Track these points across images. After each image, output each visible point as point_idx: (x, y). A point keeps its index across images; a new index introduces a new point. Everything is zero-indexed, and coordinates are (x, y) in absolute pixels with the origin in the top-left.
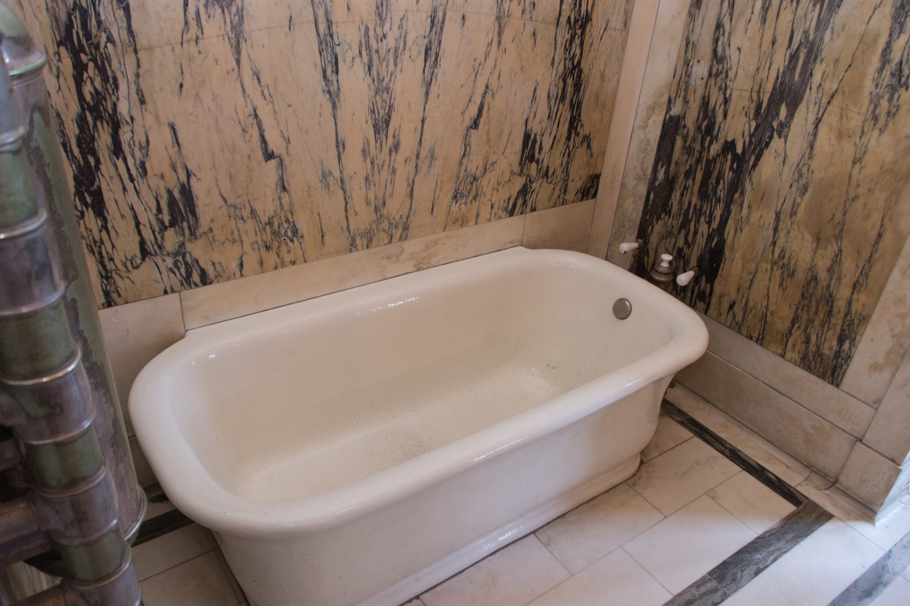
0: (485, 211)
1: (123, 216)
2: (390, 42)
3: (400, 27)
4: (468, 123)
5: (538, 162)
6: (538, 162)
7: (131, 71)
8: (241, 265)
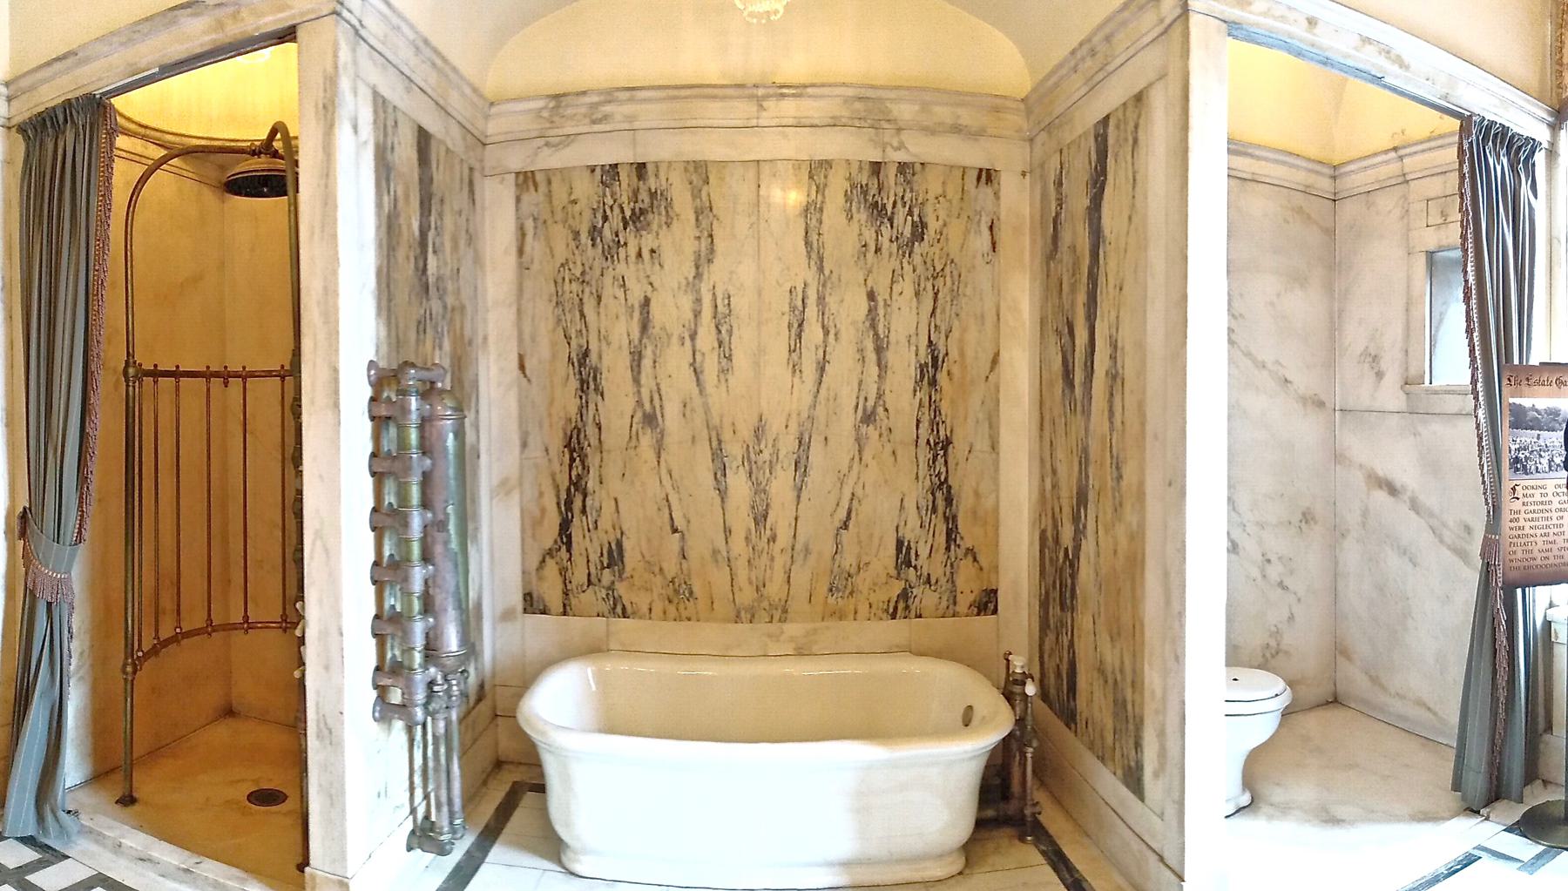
0: (863, 609)
2: (766, 456)
3: (773, 446)
4: (838, 524)
5: (915, 567)
6: (915, 567)
7: (597, 465)
8: (650, 609)
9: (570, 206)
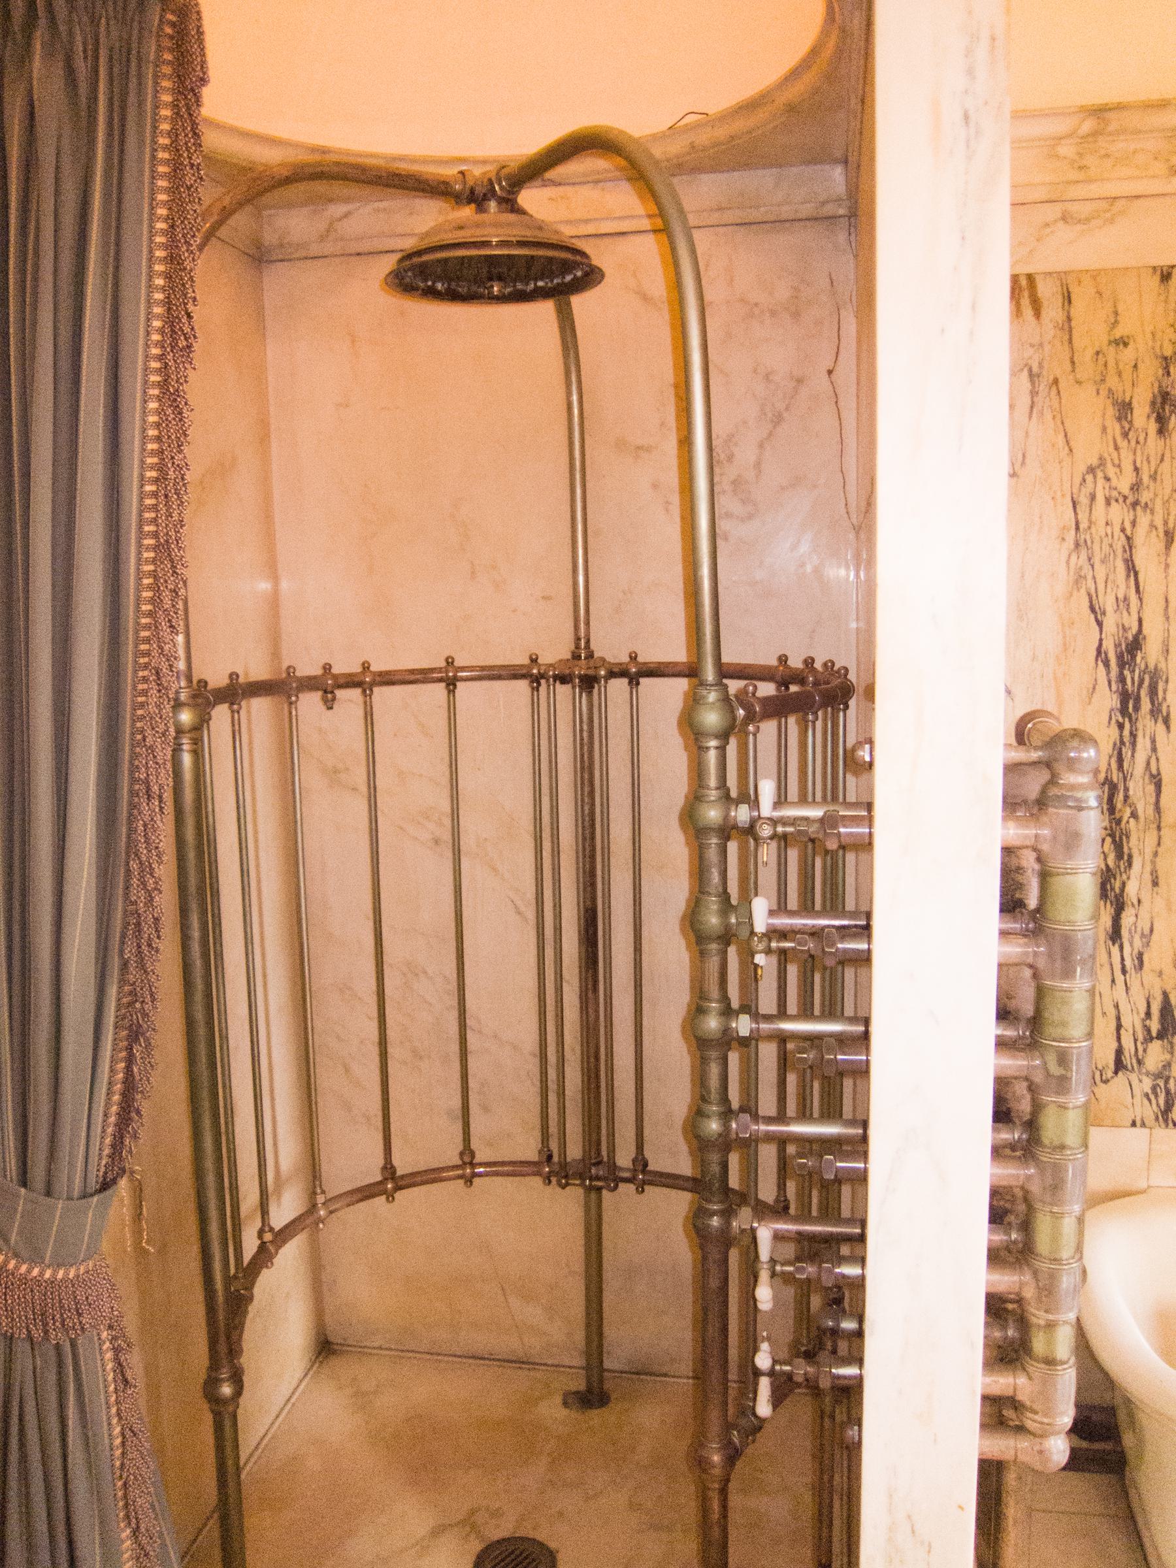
1: (1104, 1014)
7: (1149, 851)
9: (1111, 351)
